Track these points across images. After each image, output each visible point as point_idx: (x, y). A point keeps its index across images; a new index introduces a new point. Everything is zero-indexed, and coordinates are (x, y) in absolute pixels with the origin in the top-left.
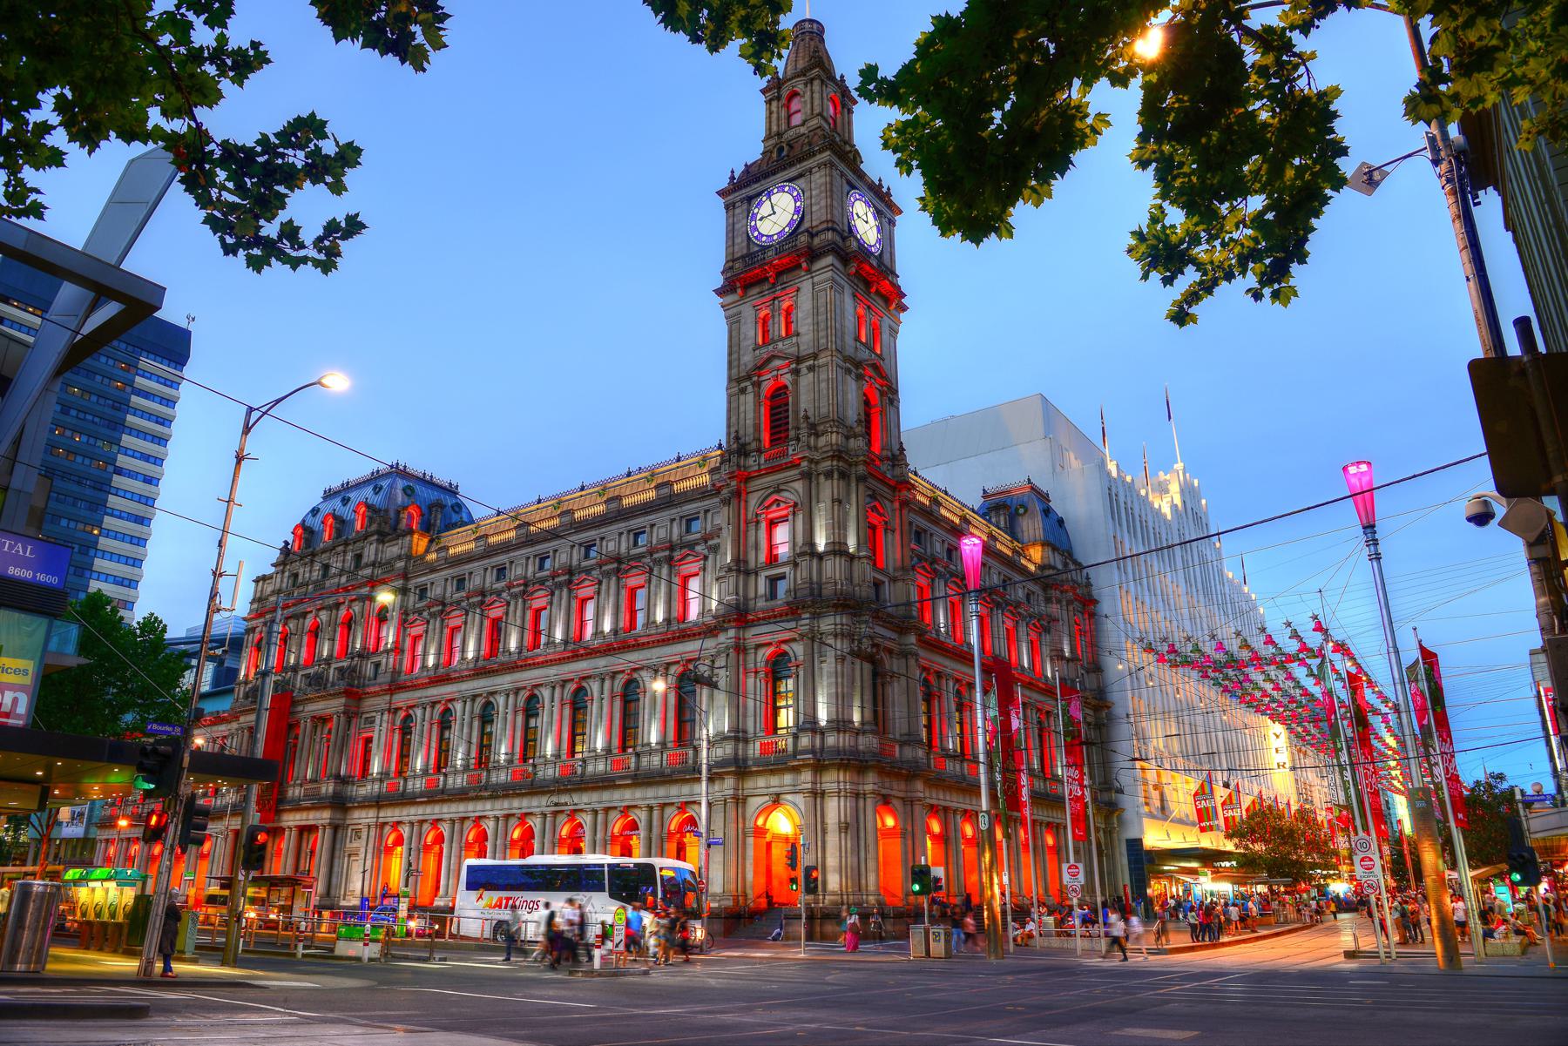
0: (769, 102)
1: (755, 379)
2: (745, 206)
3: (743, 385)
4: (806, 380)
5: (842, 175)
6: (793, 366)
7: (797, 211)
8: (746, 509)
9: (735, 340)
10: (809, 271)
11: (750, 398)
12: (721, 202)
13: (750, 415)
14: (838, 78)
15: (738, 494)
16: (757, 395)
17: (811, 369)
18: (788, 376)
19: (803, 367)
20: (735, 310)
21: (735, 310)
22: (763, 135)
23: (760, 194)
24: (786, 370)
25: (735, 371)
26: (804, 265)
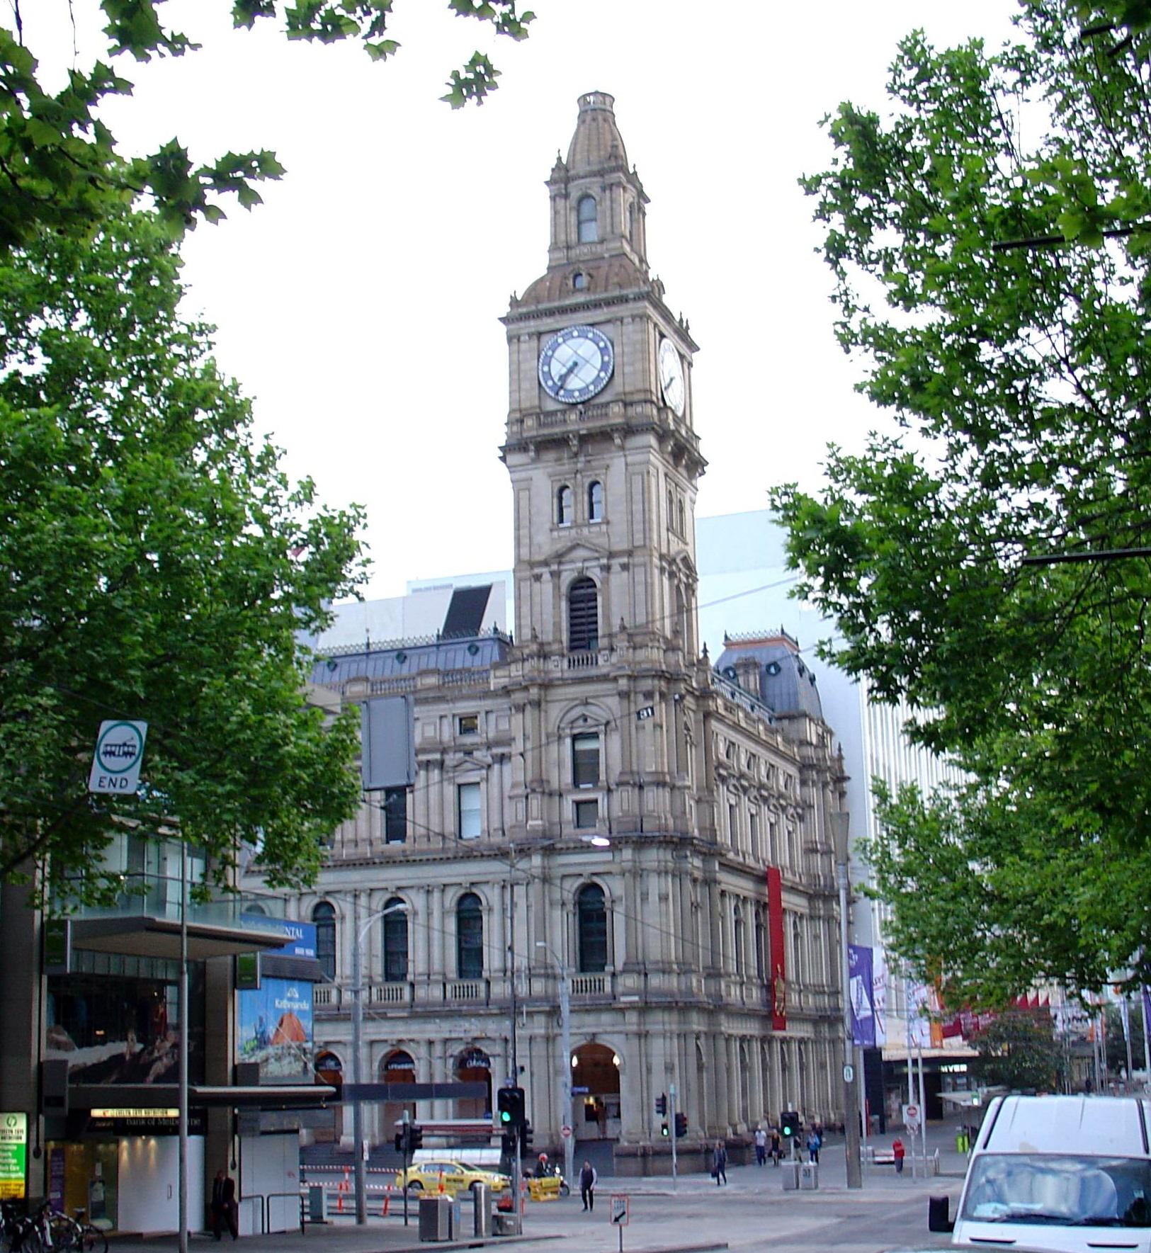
0: (553, 198)
1: (554, 567)
2: (534, 343)
3: (537, 571)
4: (618, 579)
5: (656, 325)
6: (604, 561)
7: (604, 366)
8: (546, 720)
9: (524, 513)
10: (622, 448)
11: (547, 586)
12: (503, 329)
13: (548, 609)
14: (631, 171)
15: (537, 704)
16: (557, 587)
17: (625, 567)
18: (597, 571)
19: (616, 563)
20: (523, 475)
21: (523, 475)
22: (547, 242)
23: (556, 331)
24: (594, 563)
25: (525, 552)
26: (618, 441)
